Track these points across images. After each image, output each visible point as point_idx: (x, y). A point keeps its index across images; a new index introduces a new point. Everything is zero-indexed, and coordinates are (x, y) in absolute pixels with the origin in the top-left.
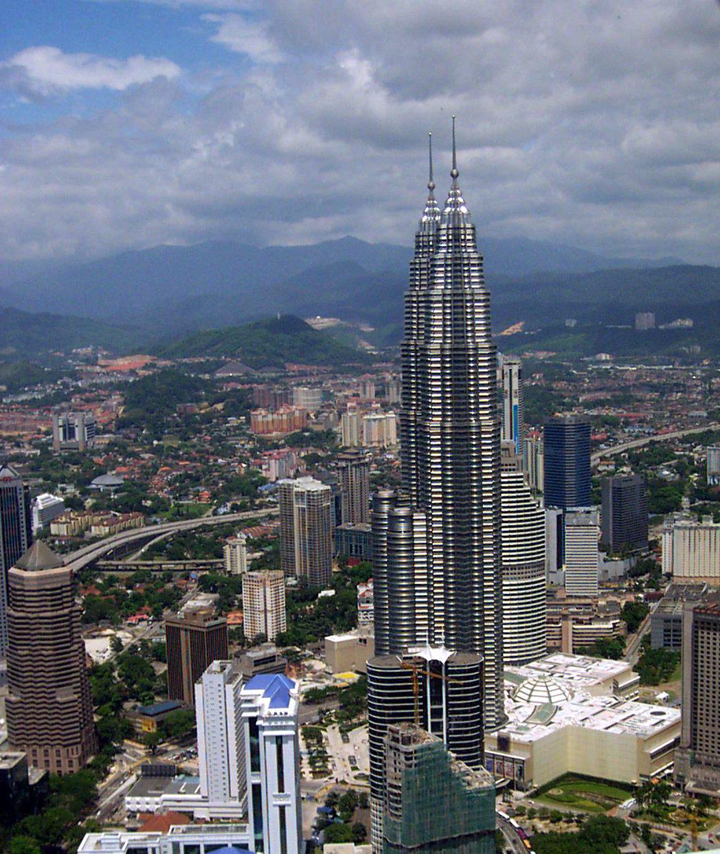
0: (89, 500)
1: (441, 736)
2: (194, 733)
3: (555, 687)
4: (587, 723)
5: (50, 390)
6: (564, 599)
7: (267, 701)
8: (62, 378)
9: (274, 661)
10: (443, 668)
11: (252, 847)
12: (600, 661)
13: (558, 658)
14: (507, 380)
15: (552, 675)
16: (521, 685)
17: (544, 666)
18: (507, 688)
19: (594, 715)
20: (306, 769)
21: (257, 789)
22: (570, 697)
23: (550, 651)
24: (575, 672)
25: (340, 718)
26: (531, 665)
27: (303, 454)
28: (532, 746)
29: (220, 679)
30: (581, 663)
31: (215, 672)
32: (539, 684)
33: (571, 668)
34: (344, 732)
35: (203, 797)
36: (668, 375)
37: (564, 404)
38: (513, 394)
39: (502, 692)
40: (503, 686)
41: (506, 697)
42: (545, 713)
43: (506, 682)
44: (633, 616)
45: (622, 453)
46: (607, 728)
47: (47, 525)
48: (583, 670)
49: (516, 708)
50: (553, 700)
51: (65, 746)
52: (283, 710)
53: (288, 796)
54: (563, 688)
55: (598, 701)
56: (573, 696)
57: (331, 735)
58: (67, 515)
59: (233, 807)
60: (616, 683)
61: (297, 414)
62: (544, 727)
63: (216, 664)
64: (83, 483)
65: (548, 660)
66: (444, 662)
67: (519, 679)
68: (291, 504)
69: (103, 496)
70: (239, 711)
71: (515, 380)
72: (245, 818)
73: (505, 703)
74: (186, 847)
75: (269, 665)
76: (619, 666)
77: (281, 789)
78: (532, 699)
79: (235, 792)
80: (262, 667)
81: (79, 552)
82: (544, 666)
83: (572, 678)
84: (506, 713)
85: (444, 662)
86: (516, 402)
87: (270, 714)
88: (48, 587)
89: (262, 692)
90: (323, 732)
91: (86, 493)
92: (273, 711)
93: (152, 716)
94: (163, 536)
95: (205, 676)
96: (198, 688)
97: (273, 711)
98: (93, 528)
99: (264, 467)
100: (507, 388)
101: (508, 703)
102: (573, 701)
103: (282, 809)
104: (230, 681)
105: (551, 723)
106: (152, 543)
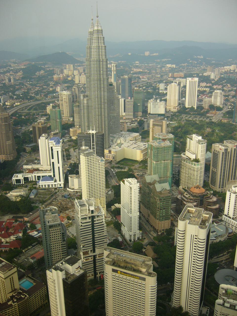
0: (15, 97)
4: (129, 147)
5: (5, 70)
6: (125, 119)
7: (55, 143)
8: (7, 67)
11: (53, 176)
14: (113, 68)
17: (120, 134)
20: (65, 158)
21: (53, 163)
25: (73, 147)
27: (66, 85)
28: (116, 152)
29: (44, 138)
31: (43, 137)
34: (74, 150)
36: (152, 67)
42: (120, 145)
44: (141, 123)
46: (133, 148)
47: (5, 103)
51: (9, 154)
52: (58, 145)
53: (60, 165)
55: (131, 142)
57: (72, 150)
58: (9, 100)
59: (49, 168)
60: (136, 138)
61: (65, 75)
63: (43, 135)
64: (13, 92)
65: (121, 133)
68: (62, 97)
69: (18, 96)
70: (49, 145)
71: (115, 68)
72: (51, 170)
73: (111, 143)
74: (38, 176)
75: (57, 135)
76: (137, 134)
77: (58, 163)
79: (49, 164)
81: (14, 109)
86: (115, 73)
88: (3, 117)
89: (53, 141)
90: (70, 150)
91: (14, 95)
93: (30, 147)
94: (32, 105)
95: (41, 138)
96: (39, 140)
97: (56, 145)
98: (16, 103)
99: (57, 88)
100: (113, 69)
102: (126, 142)
103: (59, 167)
104: (46, 139)
106: (30, 107)
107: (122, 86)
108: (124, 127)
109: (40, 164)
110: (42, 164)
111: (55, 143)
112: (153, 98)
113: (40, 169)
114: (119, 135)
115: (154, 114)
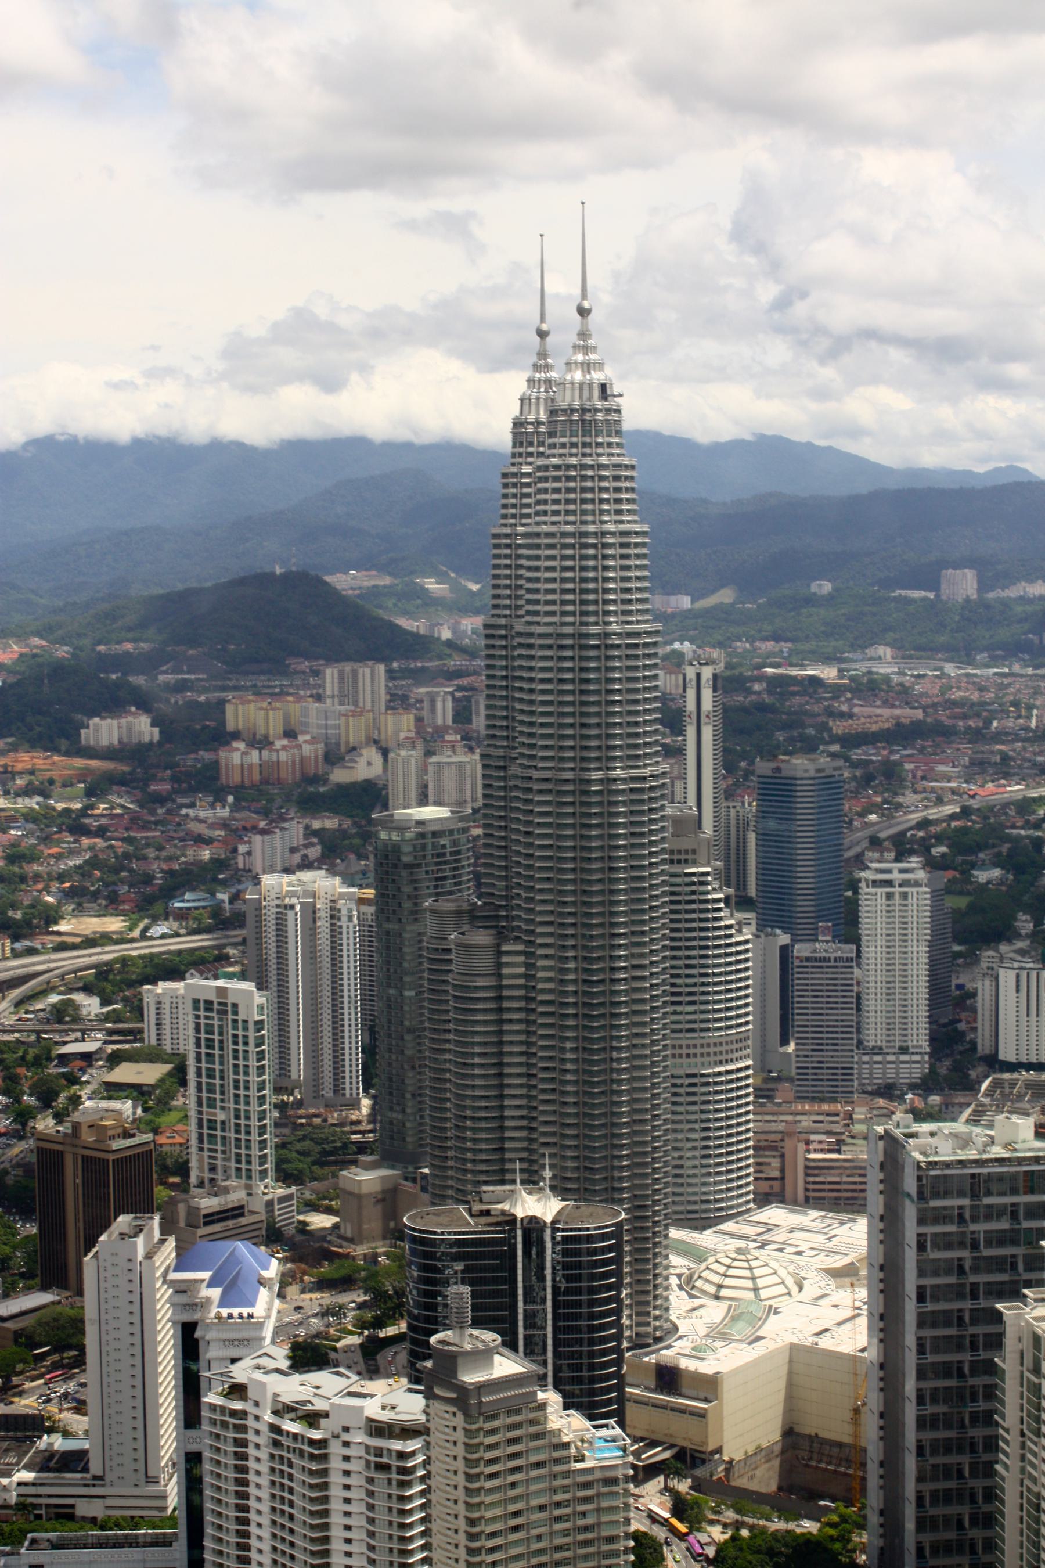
1: (545, 1363)
2: (82, 1349)
3: (766, 1270)
7: (215, 1293)
9: (242, 1215)
10: (548, 1232)
12: (854, 1221)
13: (775, 1214)
15: (763, 1245)
16: (703, 1266)
17: (749, 1230)
18: (677, 1271)
19: (839, 1324)
22: (794, 1289)
23: (763, 1200)
24: (804, 1241)
26: (726, 1226)
30: (819, 1225)
32: (736, 1264)
33: (797, 1234)
35: (95, 1478)
37: (803, 738)
38: (694, 717)
39: (667, 1278)
40: (667, 1267)
41: (676, 1288)
43: (675, 1260)
45: (911, 829)
48: (821, 1238)
49: (694, 1309)
50: (763, 1294)
52: (245, 1311)
54: (782, 1273)
56: (801, 1288)
62: (743, 1346)
63: (124, 1221)
66: (548, 1219)
67: (698, 1255)
71: (707, 694)
75: (230, 1223)
78: (724, 1292)
80: (217, 1227)
82: (749, 1230)
83: (800, 1253)
84: (673, 1318)
85: (548, 1219)
87: (219, 1317)
89: (206, 1275)
92: (225, 1312)
97: (225, 1312)
100: (691, 706)
101: (678, 1302)
105: (760, 1338)
107: (763, 838)
108: (782, 1170)
109: (85, 1469)
110: (95, 1468)
111: (215, 1293)
112: (1018, 936)
113: (84, 1509)
114: (745, 1238)
115: (1029, 1067)
